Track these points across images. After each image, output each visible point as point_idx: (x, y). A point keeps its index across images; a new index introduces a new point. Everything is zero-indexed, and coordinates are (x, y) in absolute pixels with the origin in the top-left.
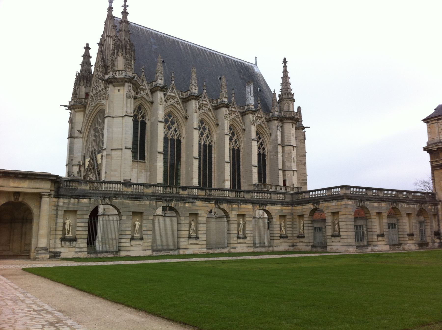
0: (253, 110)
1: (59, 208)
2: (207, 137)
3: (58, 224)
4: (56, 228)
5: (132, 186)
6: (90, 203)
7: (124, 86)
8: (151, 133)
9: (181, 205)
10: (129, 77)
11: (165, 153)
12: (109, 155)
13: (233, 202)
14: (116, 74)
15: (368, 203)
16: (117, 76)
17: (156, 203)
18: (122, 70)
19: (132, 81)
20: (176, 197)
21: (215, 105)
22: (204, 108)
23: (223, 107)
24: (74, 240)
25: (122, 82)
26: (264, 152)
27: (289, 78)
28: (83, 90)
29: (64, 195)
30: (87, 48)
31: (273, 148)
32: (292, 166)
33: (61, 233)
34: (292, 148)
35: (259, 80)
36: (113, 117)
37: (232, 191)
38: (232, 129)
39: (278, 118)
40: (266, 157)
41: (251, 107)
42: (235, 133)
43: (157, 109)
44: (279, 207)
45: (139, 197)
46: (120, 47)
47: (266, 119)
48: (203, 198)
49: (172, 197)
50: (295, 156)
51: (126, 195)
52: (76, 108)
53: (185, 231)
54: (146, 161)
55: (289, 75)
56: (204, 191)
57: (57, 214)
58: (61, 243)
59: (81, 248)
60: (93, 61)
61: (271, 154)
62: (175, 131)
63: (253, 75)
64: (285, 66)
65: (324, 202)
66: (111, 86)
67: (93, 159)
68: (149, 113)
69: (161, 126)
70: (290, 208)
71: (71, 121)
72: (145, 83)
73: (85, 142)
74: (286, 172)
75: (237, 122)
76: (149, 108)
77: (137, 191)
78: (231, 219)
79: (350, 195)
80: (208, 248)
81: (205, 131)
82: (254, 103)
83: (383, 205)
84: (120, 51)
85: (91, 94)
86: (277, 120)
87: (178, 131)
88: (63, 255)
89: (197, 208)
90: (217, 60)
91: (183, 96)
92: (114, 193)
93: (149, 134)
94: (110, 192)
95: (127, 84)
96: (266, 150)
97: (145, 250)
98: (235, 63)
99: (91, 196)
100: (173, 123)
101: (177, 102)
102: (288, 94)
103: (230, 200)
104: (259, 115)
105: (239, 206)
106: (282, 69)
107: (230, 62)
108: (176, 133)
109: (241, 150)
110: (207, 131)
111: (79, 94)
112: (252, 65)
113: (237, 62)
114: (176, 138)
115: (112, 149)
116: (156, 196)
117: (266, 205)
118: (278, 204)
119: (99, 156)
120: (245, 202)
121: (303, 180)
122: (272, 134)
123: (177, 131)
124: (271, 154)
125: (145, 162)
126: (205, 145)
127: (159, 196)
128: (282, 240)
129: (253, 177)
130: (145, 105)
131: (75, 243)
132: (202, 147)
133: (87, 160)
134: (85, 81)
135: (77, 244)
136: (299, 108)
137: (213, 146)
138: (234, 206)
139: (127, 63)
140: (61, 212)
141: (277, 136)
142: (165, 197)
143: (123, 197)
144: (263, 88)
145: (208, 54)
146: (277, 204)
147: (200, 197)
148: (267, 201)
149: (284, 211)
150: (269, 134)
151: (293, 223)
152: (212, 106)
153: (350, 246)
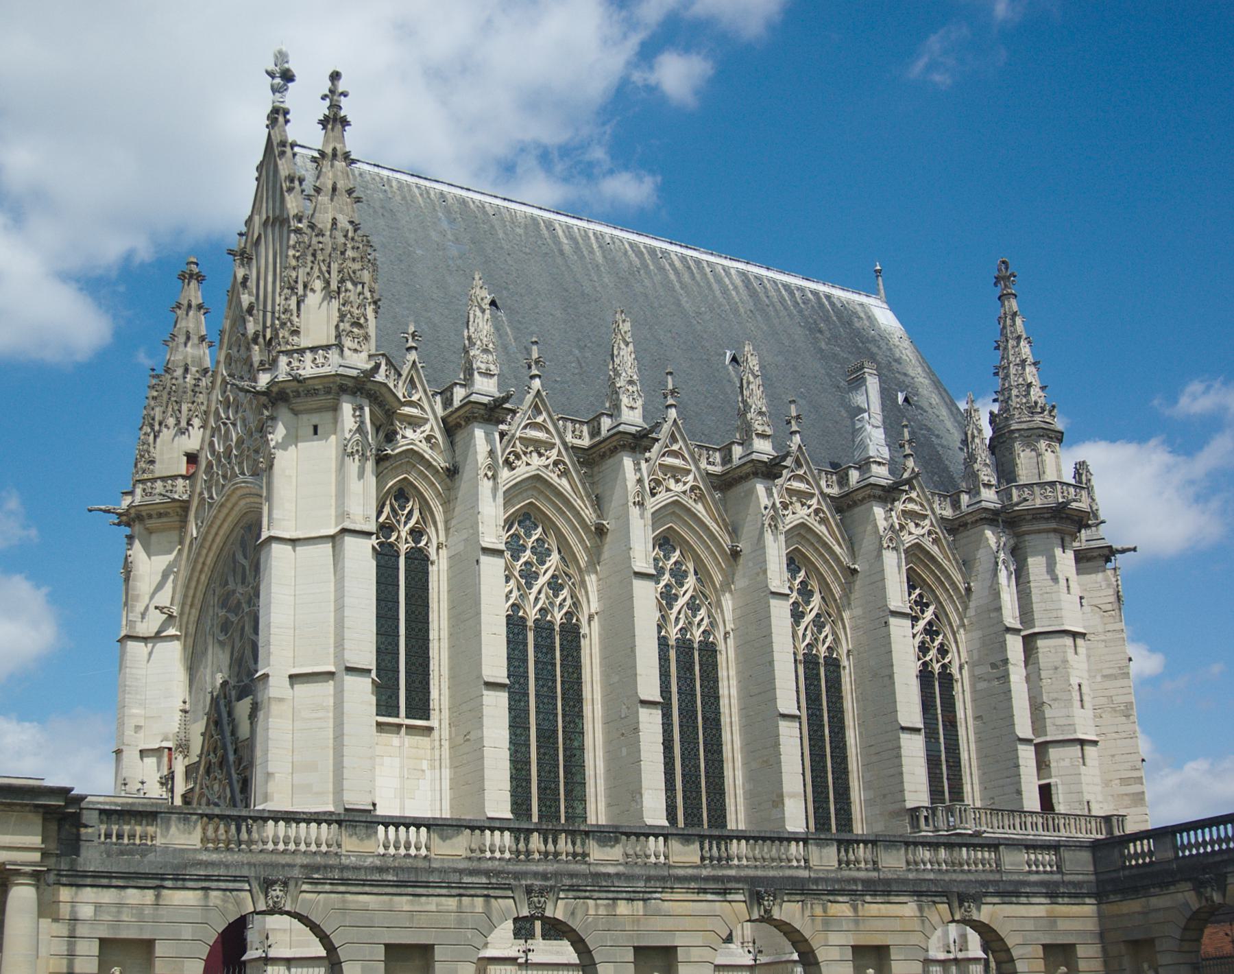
0: (883, 482)
5: (381, 828)
9: (594, 908)
10: (354, 373)
11: (515, 689)
13: (832, 892)
16: (308, 370)
17: (487, 904)
19: (369, 386)
20: (572, 875)
26: (944, 666)
32: (1077, 720)
35: (898, 361)
37: (822, 843)
39: (995, 512)
40: (957, 687)
41: (874, 468)
42: (814, 585)
43: (475, 496)
44: (1039, 909)
45: (409, 878)
49: (556, 874)
50: (1086, 675)
51: (356, 868)
56: (697, 845)
63: (874, 341)
69: (492, 571)
77: (402, 851)
82: (886, 453)
89: (669, 923)
90: (715, 286)
92: (306, 861)
94: (287, 859)
98: (792, 293)
100: (542, 555)
101: (556, 463)
103: (816, 881)
104: (911, 506)
105: (855, 909)
107: (772, 293)
108: (557, 596)
114: (558, 616)
115: (291, 677)
116: (487, 873)
117: (978, 899)
118: (1035, 894)
120: (883, 889)
126: (684, 646)
127: (498, 873)
129: (906, 778)
132: (673, 654)
137: (721, 646)
138: (834, 909)
141: (997, 595)
142: (524, 875)
143: (345, 882)
145: (677, 264)
146: (1027, 895)
147: (681, 872)
148: (984, 883)
149: (1062, 925)
150: (962, 587)
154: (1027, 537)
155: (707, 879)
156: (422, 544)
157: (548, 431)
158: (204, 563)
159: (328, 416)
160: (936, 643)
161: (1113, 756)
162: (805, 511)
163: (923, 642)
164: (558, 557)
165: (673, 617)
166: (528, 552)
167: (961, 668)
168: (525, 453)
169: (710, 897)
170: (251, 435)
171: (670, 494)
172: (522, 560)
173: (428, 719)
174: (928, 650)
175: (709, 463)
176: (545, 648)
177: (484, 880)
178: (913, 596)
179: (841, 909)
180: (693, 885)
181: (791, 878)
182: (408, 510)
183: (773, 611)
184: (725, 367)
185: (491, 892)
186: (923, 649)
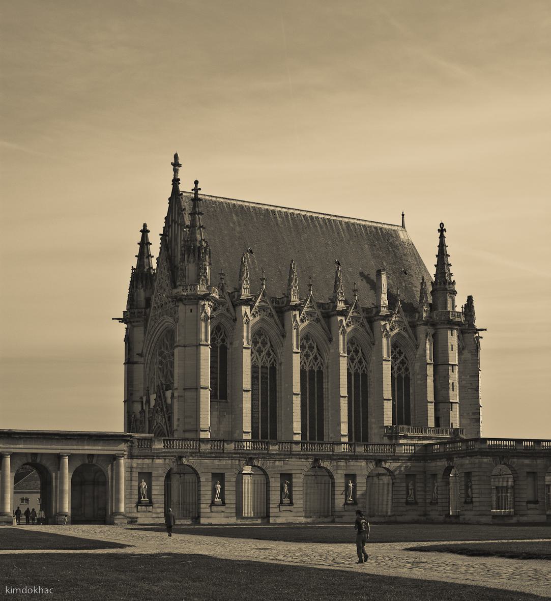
0: (384, 314)
1: (134, 470)
2: (316, 358)
3: (133, 488)
4: (131, 492)
6: (165, 464)
9: (269, 463)
12: (181, 396)
13: (339, 459)
15: (515, 460)
20: (263, 454)
24: (151, 503)
25: (195, 299)
27: (448, 256)
28: (142, 294)
29: (137, 456)
30: (145, 231)
33: (137, 497)
34: (450, 368)
46: (192, 251)
47: (409, 322)
48: (298, 455)
52: (134, 322)
53: (275, 495)
54: (229, 400)
55: (449, 251)
57: (131, 476)
58: (137, 508)
59: (158, 513)
60: (155, 249)
63: (396, 247)
64: (442, 237)
65: (458, 459)
67: (161, 397)
70: (422, 464)
71: (128, 339)
73: (148, 369)
74: (441, 404)
78: (336, 481)
79: (488, 450)
80: (305, 517)
81: (312, 352)
83: (539, 461)
85: (153, 304)
88: (140, 521)
89: (290, 467)
97: (228, 517)
98: (366, 230)
99: (165, 456)
100: (264, 344)
103: (335, 455)
105: (346, 463)
111: (137, 301)
112: (396, 228)
113: (370, 227)
115: (184, 389)
116: (239, 454)
117: (385, 461)
119: (168, 394)
121: (474, 414)
123: (270, 355)
125: (227, 402)
127: (242, 454)
128: (409, 507)
131: (151, 507)
133: (153, 397)
134: (144, 282)
135: (154, 509)
136: (470, 298)
138: (339, 463)
140: (135, 475)
141: (425, 350)
142: (250, 454)
143: (201, 457)
144: (411, 269)
145: (321, 222)
147: (295, 453)
151: (425, 485)
153: (484, 515)
154: (439, 330)
155: (302, 455)
156: (225, 344)
157: (267, 303)
158: (153, 340)
160: (405, 366)
161: (471, 405)
166: (260, 343)
169: (303, 460)
172: (258, 346)
173: (226, 399)
177: (239, 456)
179: (342, 463)
180: (298, 457)
181: (328, 454)
183: (341, 362)
185: (241, 459)
186: (399, 369)
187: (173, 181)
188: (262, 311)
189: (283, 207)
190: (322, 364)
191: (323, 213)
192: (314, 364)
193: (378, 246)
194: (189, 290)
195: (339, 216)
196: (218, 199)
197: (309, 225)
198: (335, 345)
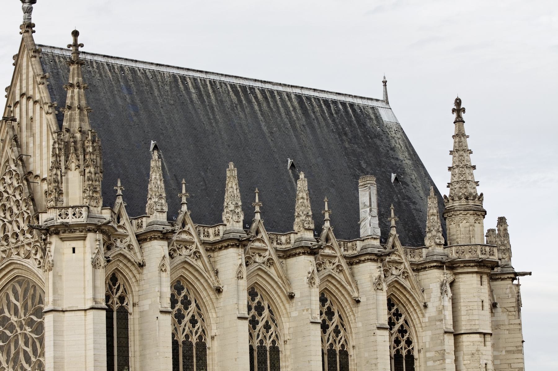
0: (376, 251)
2: (267, 327)
7: (85, 240)
8: (142, 336)
14: (67, 215)
16: (71, 220)
18: (82, 207)
21: (284, 247)
22: (258, 259)
23: (304, 253)
25: (82, 232)
26: (409, 351)
31: (432, 339)
35: (393, 149)
36: (63, 311)
38: (326, 300)
40: (416, 363)
47: (412, 264)
50: (490, 358)
55: (470, 143)
61: (429, 355)
62: (193, 322)
63: (378, 136)
64: (459, 121)
66: (54, 239)
68: (135, 288)
72: (125, 219)
75: (339, 282)
76: (135, 276)
84: (72, 157)
86: (440, 267)
87: (200, 321)
90: (282, 110)
91: (208, 236)
93: (137, 337)
95: (90, 236)
96: (415, 344)
98: (328, 106)
101: (195, 253)
102: (467, 198)
106: (452, 129)
109: (351, 352)
110: (266, 313)
112: (374, 104)
113: (335, 102)
122: (429, 305)
123: (197, 322)
124: (429, 355)
130: (126, 271)
136: (502, 221)
139: (89, 186)
141: (441, 311)
145: (259, 96)
150: (421, 305)
152: (277, 250)
156: (125, 304)
157: (190, 234)
159: (80, 243)
160: (405, 338)
162: (332, 267)
163: (397, 338)
164: (195, 304)
165: (256, 334)
166: (179, 304)
167: (419, 351)
168: (178, 249)
170: (24, 234)
171: (257, 264)
172: (177, 308)
174: (400, 342)
175: (278, 244)
176: (188, 357)
178: (393, 311)
182: (117, 285)
184: (287, 171)
186: (397, 342)
187: (21, 27)
188: (184, 248)
189: (198, 71)
190: (277, 336)
191: (260, 79)
192: (265, 337)
193: (350, 135)
194: (70, 215)
195: (285, 85)
196: (96, 58)
197: (240, 101)
198: (299, 304)
